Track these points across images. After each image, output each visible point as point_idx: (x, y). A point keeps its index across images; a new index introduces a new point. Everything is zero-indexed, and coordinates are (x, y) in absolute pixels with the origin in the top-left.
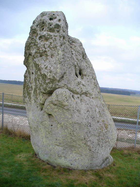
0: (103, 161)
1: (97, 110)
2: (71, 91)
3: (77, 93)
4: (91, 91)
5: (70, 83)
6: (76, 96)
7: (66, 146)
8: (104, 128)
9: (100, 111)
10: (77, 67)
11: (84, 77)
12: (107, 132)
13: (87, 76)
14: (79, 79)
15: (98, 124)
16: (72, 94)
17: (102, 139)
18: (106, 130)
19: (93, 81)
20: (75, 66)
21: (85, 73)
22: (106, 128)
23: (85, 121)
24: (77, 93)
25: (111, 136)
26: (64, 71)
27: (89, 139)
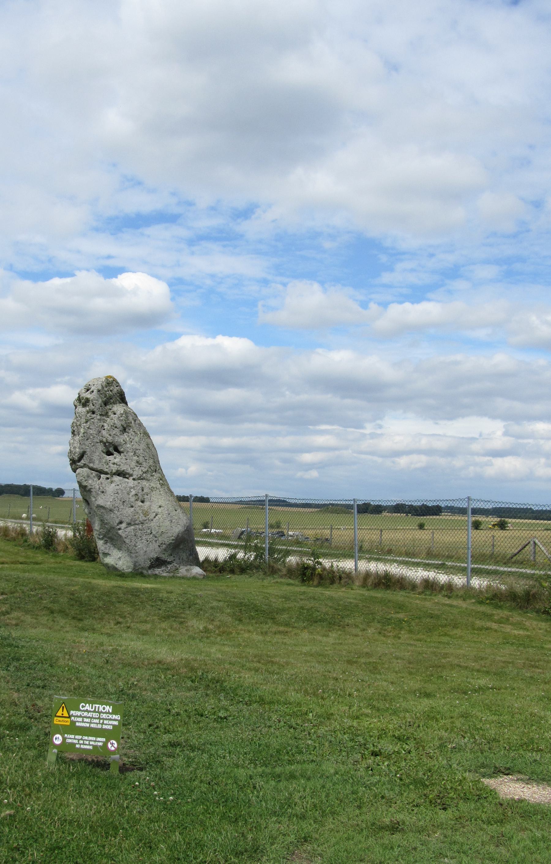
0: (150, 561)
1: (133, 492)
2: (97, 471)
3: (106, 473)
4: (130, 471)
5: (93, 463)
6: (102, 476)
7: (106, 539)
8: (142, 515)
9: (139, 495)
10: (107, 444)
11: (122, 454)
12: (147, 521)
13: (125, 453)
14: (116, 458)
15: (132, 509)
16: (94, 473)
17: (140, 529)
18: (144, 518)
19: (135, 458)
20: (105, 444)
21: (122, 450)
22: (146, 514)
23: (109, 503)
24: (106, 473)
25: (157, 528)
26: (82, 450)
27: (118, 527)
